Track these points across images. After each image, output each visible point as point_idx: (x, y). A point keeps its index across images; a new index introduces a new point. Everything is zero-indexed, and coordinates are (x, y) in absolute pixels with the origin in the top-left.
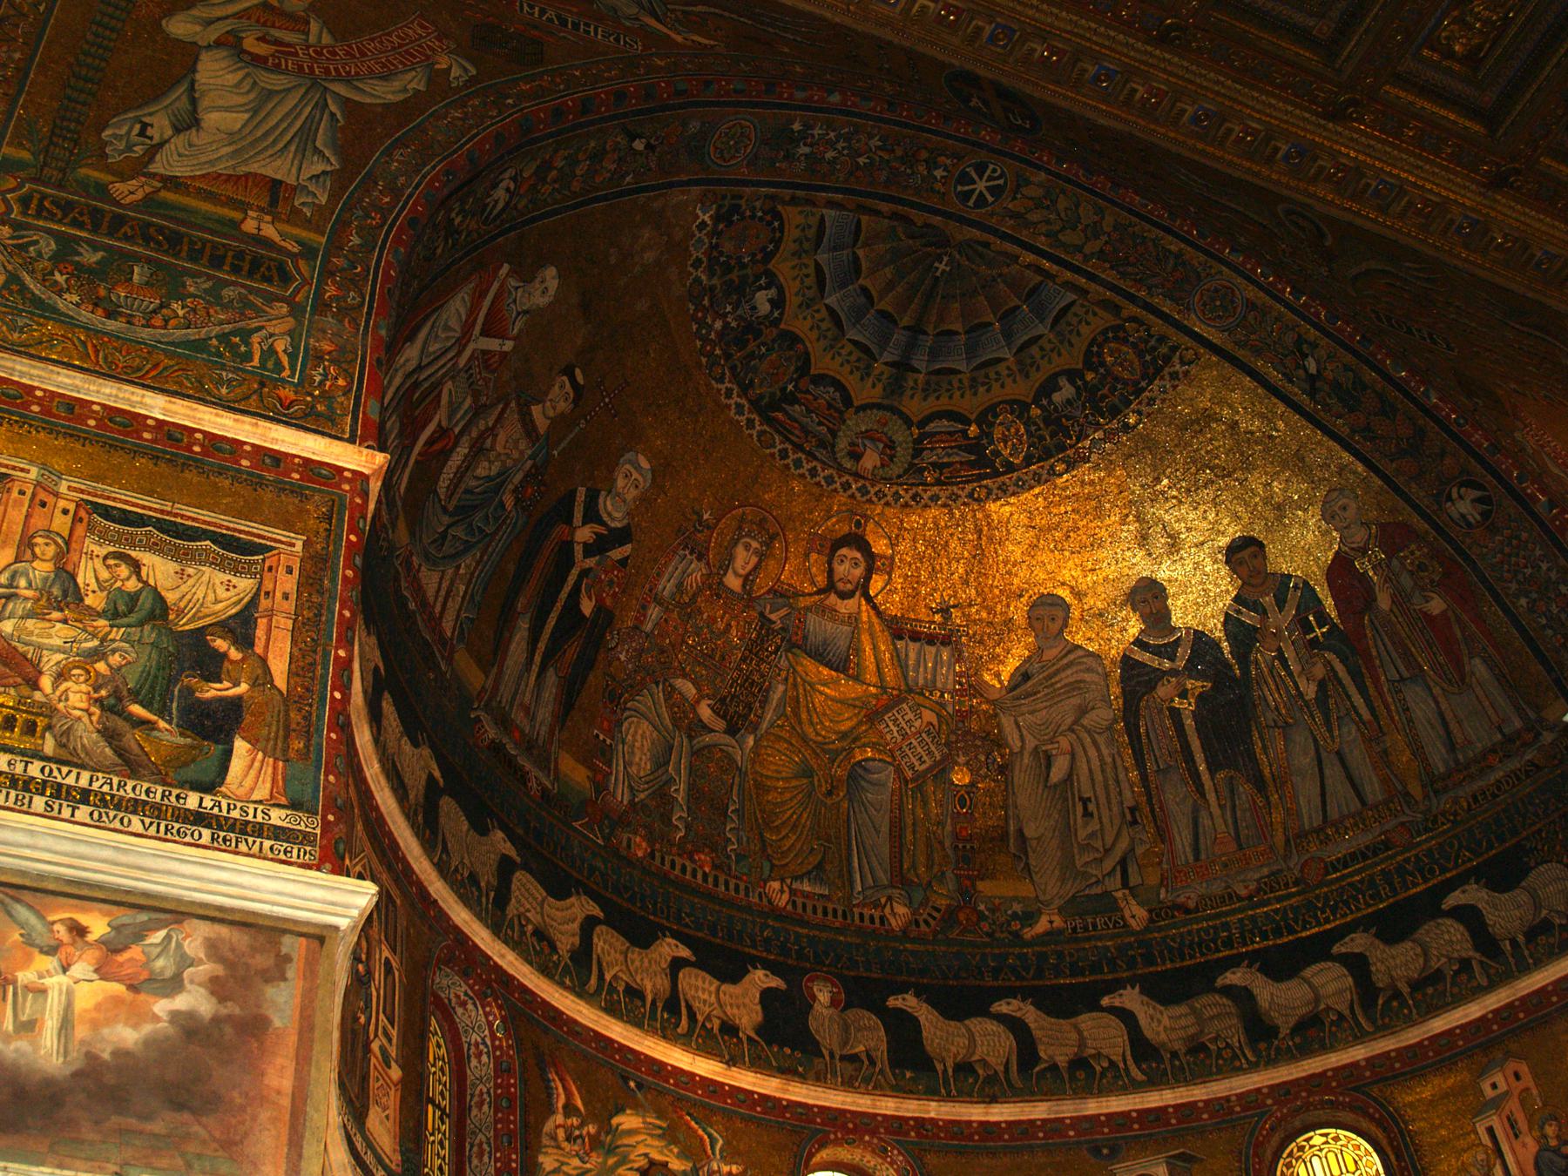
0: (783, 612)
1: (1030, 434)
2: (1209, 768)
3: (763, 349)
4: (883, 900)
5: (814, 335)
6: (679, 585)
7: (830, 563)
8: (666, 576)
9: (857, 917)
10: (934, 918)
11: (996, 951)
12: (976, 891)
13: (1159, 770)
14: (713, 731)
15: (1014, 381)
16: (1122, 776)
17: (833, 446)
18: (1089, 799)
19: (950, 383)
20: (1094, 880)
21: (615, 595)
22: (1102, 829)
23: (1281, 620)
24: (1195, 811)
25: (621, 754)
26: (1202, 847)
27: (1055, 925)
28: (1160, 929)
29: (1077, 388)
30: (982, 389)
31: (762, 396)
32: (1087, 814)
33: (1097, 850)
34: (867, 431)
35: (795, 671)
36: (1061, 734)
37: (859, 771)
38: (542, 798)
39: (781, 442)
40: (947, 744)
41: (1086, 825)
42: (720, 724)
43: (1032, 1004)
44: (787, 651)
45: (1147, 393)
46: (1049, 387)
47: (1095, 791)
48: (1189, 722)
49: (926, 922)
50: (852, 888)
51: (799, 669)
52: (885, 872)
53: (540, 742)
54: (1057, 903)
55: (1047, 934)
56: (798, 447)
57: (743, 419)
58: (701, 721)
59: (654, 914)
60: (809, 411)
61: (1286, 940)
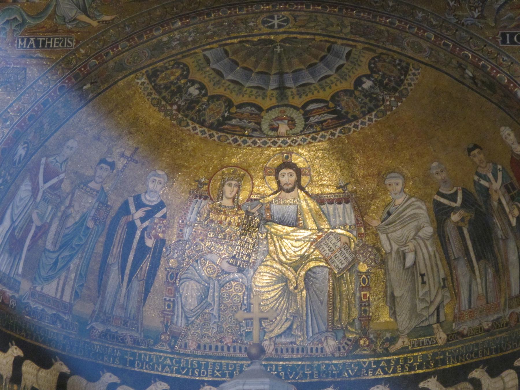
0: (258, 207)
1: (360, 103)
2: (476, 258)
3: (204, 106)
4: (323, 339)
5: (228, 92)
6: (198, 212)
7: (277, 178)
8: (189, 213)
9: (309, 349)
10: (348, 345)
11: (376, 359)
12: (368, 327)
13: (455, 259)
14: (229, 273)
15: (341, 82)
16: (439, 263)
17: (260, 129)
18: (424, 275)
19: (309, 88)
20: (424, 318)
21: (164, 232)
22: (430, 290)
23: (497, 185)
24: (470, 281)
25: (180, 303)
26: (472, 301)
27: (405, 343)
28: (451, 345)
29: (373, 81)
30: (327, 89)
31: (212, 124)
32: (424, 283)
33: (428, 302)
34: (276, 118)
35: (271, 233)
36: (409, 242)
37: (309, 273)
38: (134, 343)
39: (232, 137)
40: (355, 253)
41: (423, 288)
42: (235, 269)
43: (389, 387)
44: (265, 223)
45: (406, 82)
46: (359, 82)
47: (427, 270)
48: (467, 236)
49: (343, 347)
50: (307, 335)
51: (272, 230)
52: (325, 325)
53: (132, 317)
54: (407, 332)
55: (402, 348)
56: (244, 135)
57: (207, 135)
58: (223, 270)
59: (199, 376)
60: (241, 119)
61: (499, 355)
